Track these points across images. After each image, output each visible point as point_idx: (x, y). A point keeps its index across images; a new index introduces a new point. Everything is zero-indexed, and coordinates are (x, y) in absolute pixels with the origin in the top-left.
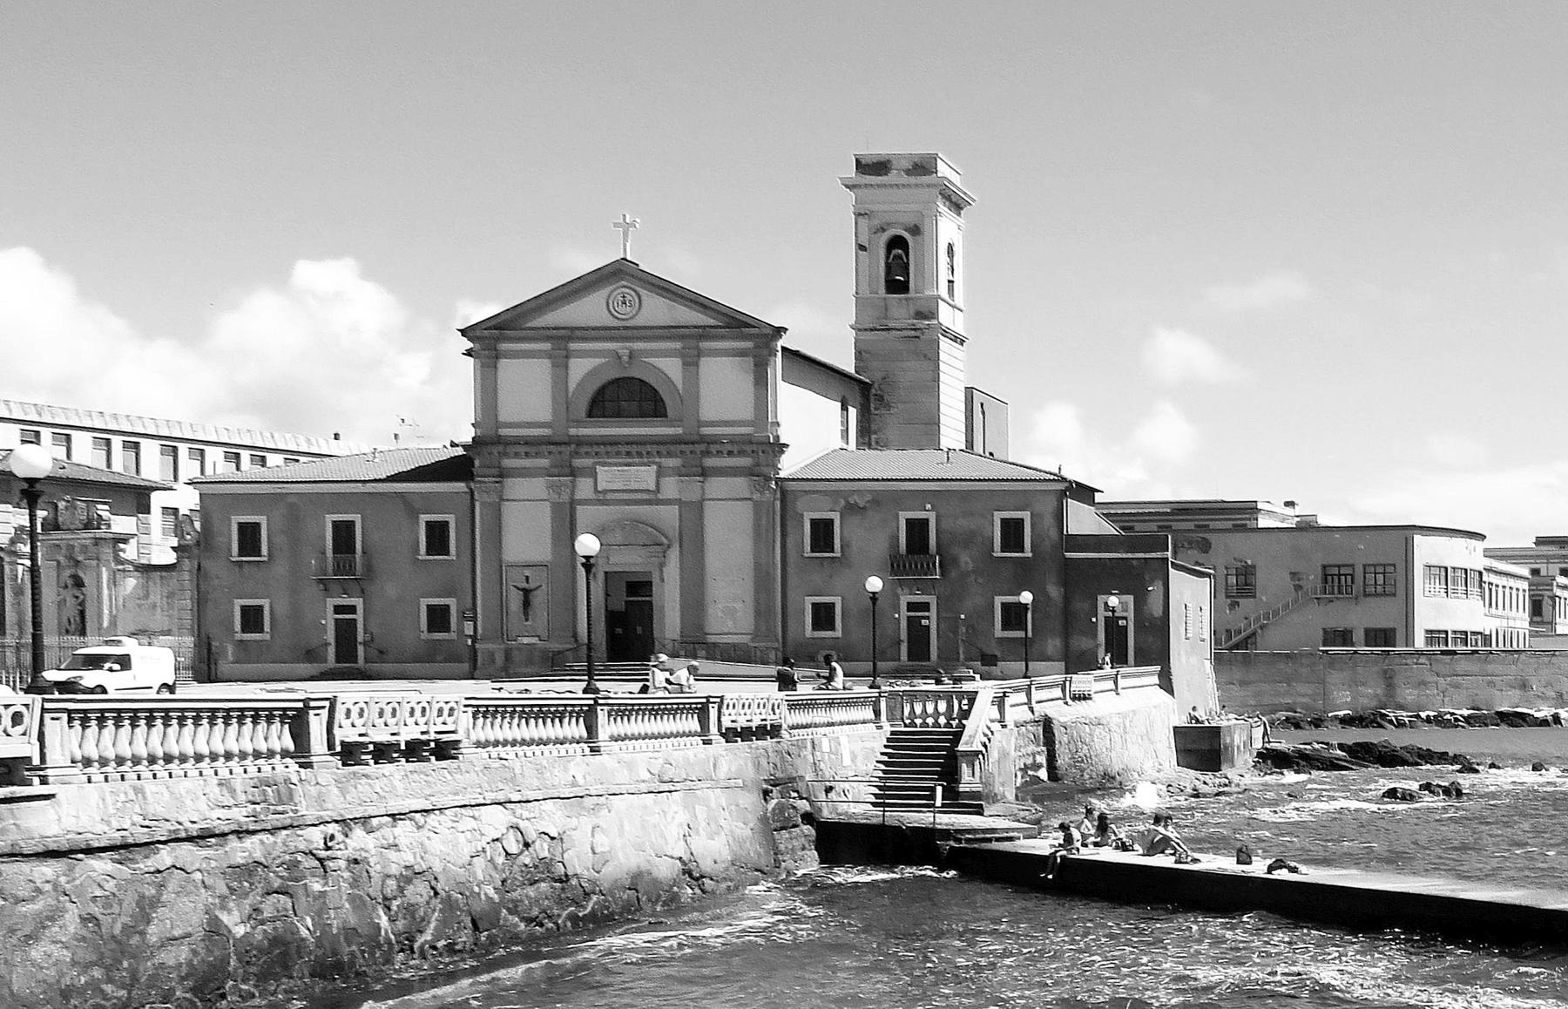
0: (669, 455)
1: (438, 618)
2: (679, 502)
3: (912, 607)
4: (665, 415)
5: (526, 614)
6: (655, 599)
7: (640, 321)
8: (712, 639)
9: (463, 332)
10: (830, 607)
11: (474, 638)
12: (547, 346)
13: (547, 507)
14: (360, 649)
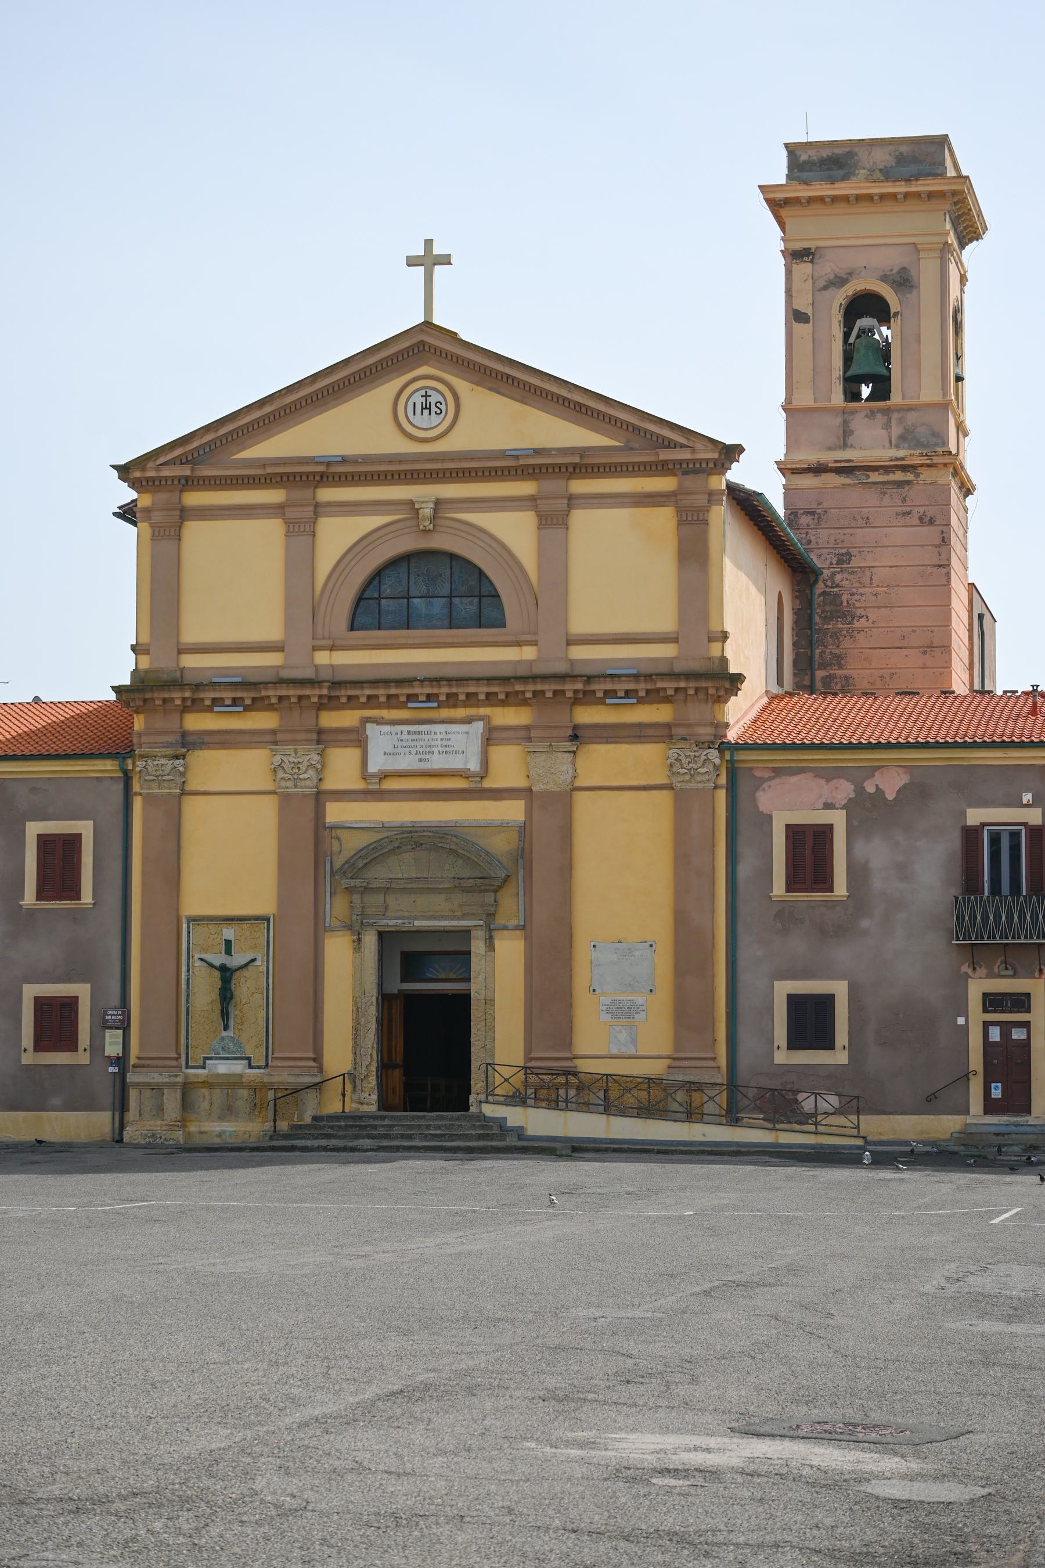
0: (512, 699)
1: (56, 1023)
2: (527, 793)
3: (992, 1002)
4: (500, 623)
5: (225, 1015)
6: (476, 988)
7: (460, 441)
8: (586, 1066)
9: (124, 471)
10: (826, 1002)
11: (121, 1061)
12: (274, 496)
13: (267, 809)
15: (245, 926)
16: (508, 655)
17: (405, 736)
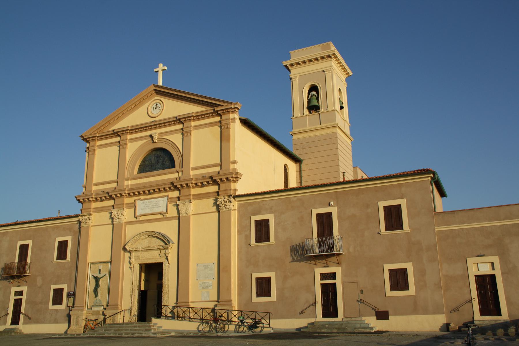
4: (173, 166)
14: (22, 317)
15: (105, 264)
16: (176, 175)
17: (147, 203)
